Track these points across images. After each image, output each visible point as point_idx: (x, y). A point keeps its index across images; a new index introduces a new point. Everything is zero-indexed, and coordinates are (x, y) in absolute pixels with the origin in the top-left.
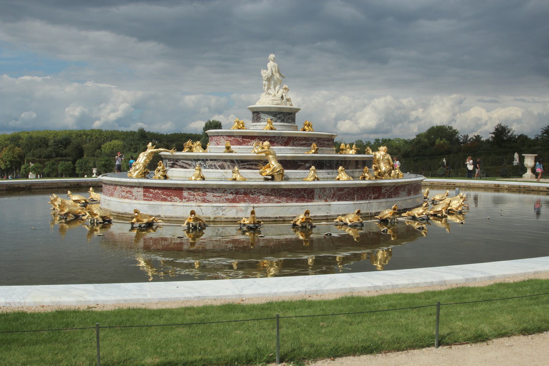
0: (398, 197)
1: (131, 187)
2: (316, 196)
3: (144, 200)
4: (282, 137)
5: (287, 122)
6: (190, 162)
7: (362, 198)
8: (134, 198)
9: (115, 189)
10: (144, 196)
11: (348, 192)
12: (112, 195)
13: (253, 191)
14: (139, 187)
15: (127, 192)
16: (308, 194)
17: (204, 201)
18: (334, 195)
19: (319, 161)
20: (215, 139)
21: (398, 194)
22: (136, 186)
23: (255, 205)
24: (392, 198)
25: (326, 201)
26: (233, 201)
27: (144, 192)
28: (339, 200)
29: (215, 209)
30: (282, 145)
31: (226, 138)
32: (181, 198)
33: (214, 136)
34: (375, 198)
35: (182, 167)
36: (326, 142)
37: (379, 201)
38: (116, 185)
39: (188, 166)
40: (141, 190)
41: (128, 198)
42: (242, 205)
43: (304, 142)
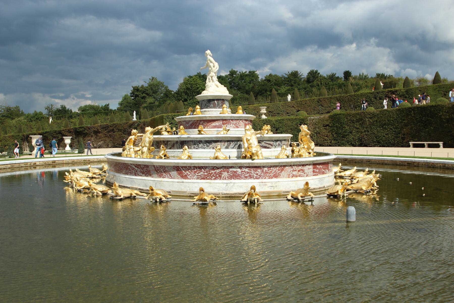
1: (303, 165)
3: (314, 175)
6: (271, 143)
8: (305, 175)
9: (283, 170)
10: (314, 172)
12: (276, 176)
14: (309, 165)
15: (299, 171)
20: (235, 122)
22: (307, 165)
27: (314, 168)
31: (244, 121)
33: (232, 120)
35: (265, 147)
38: (285, 166)
39: (270, 147)
40: (311, 167)
41: (300, 176)
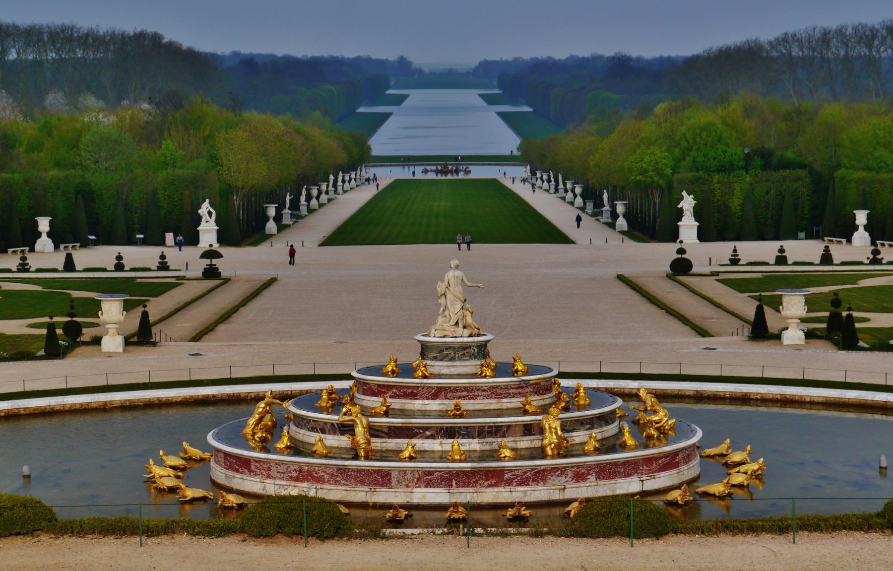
0: (544, 485)
2: (394, 481)
4: (428, 388)
5: (459, 360)
7: (465, 485)
11: (441, 476)
13: (317, 469)
16: (382, 478)
17: (269, 477)
18: (419, 479)
19: (447, 428)
21: (543, 480)
23: (319, 486)
24: (528, 485)
25: (407, 486)
26: (297, 479)
28: (426, 487)
29: (277, 487)
30: (428, 399)
32: (250, 471)
34: (489, 486)
36: (512, 391)
37: (496, 489)
42: (305, 485)
43: (464, 393)
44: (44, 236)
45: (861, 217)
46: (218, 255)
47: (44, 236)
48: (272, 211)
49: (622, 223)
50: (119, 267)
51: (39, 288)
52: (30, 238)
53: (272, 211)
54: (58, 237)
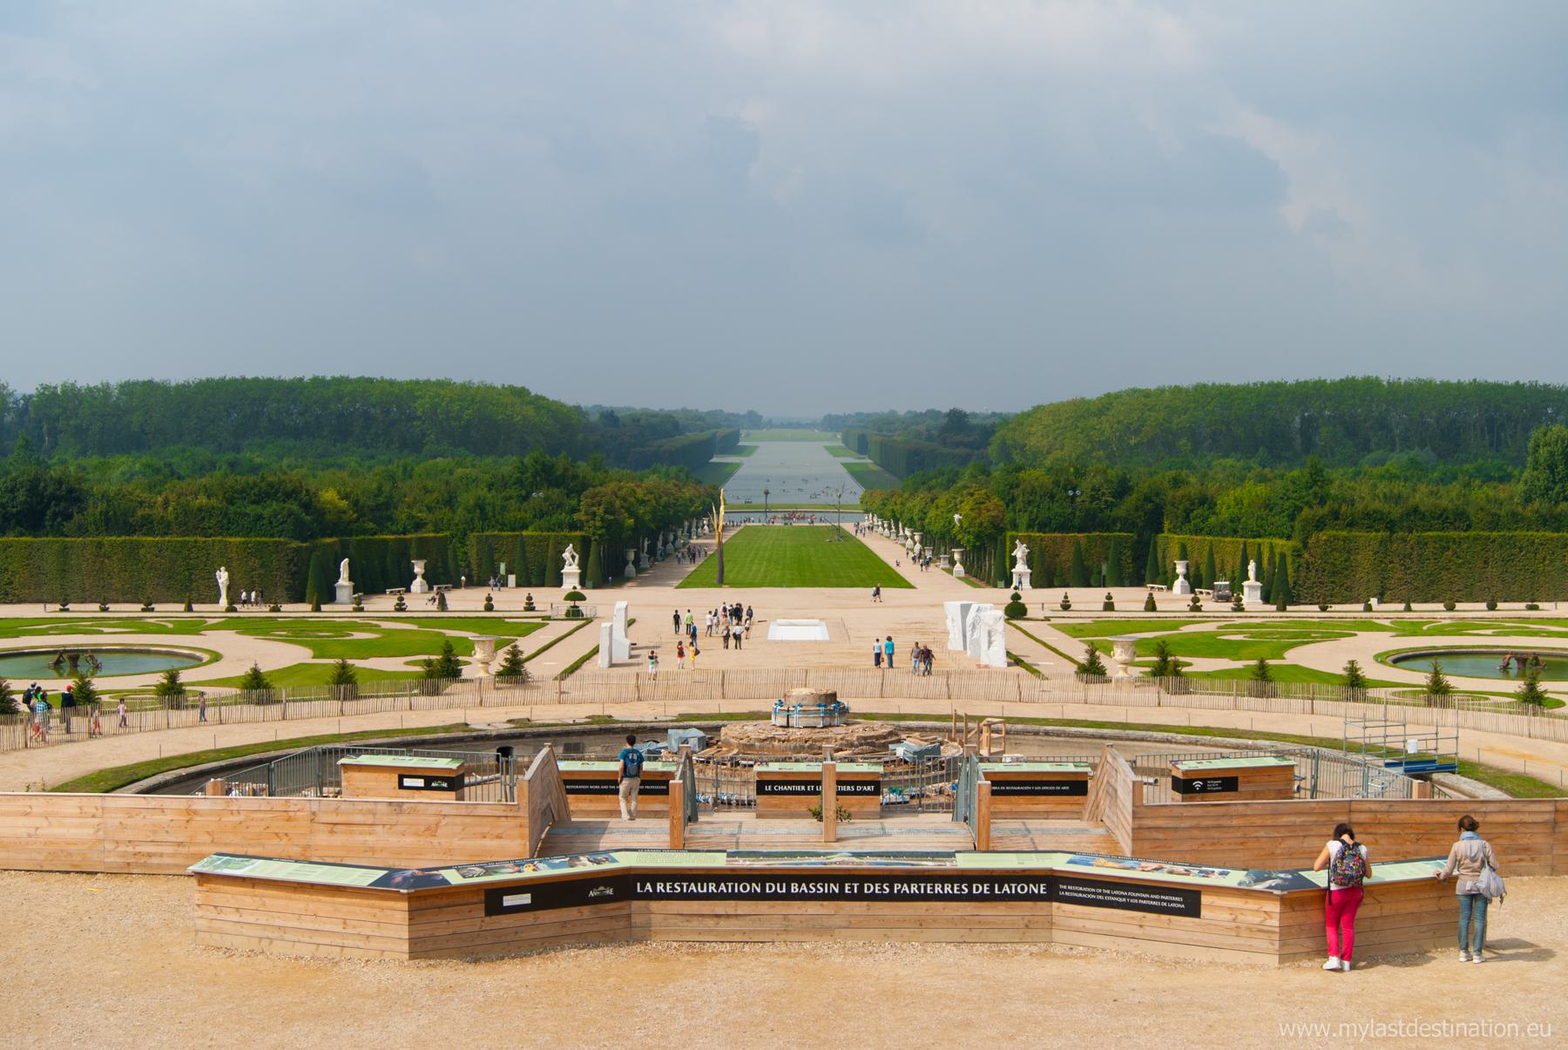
44: (419, 579)
45: (1180, 569)
46: (583, 598)
47: (419, 579)
48: (631, 556)
49: (959, 568)
50: (489, 608)
51: (414, 627)
52: (406, 581)
53: (631, 556)
54: (431, 579)
